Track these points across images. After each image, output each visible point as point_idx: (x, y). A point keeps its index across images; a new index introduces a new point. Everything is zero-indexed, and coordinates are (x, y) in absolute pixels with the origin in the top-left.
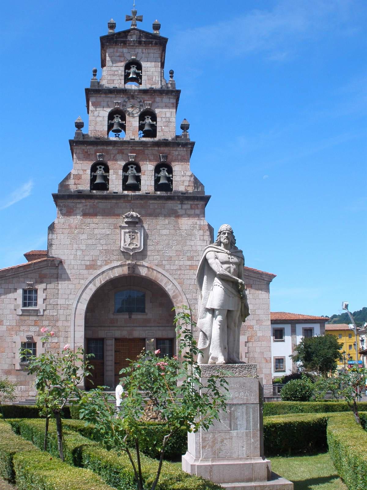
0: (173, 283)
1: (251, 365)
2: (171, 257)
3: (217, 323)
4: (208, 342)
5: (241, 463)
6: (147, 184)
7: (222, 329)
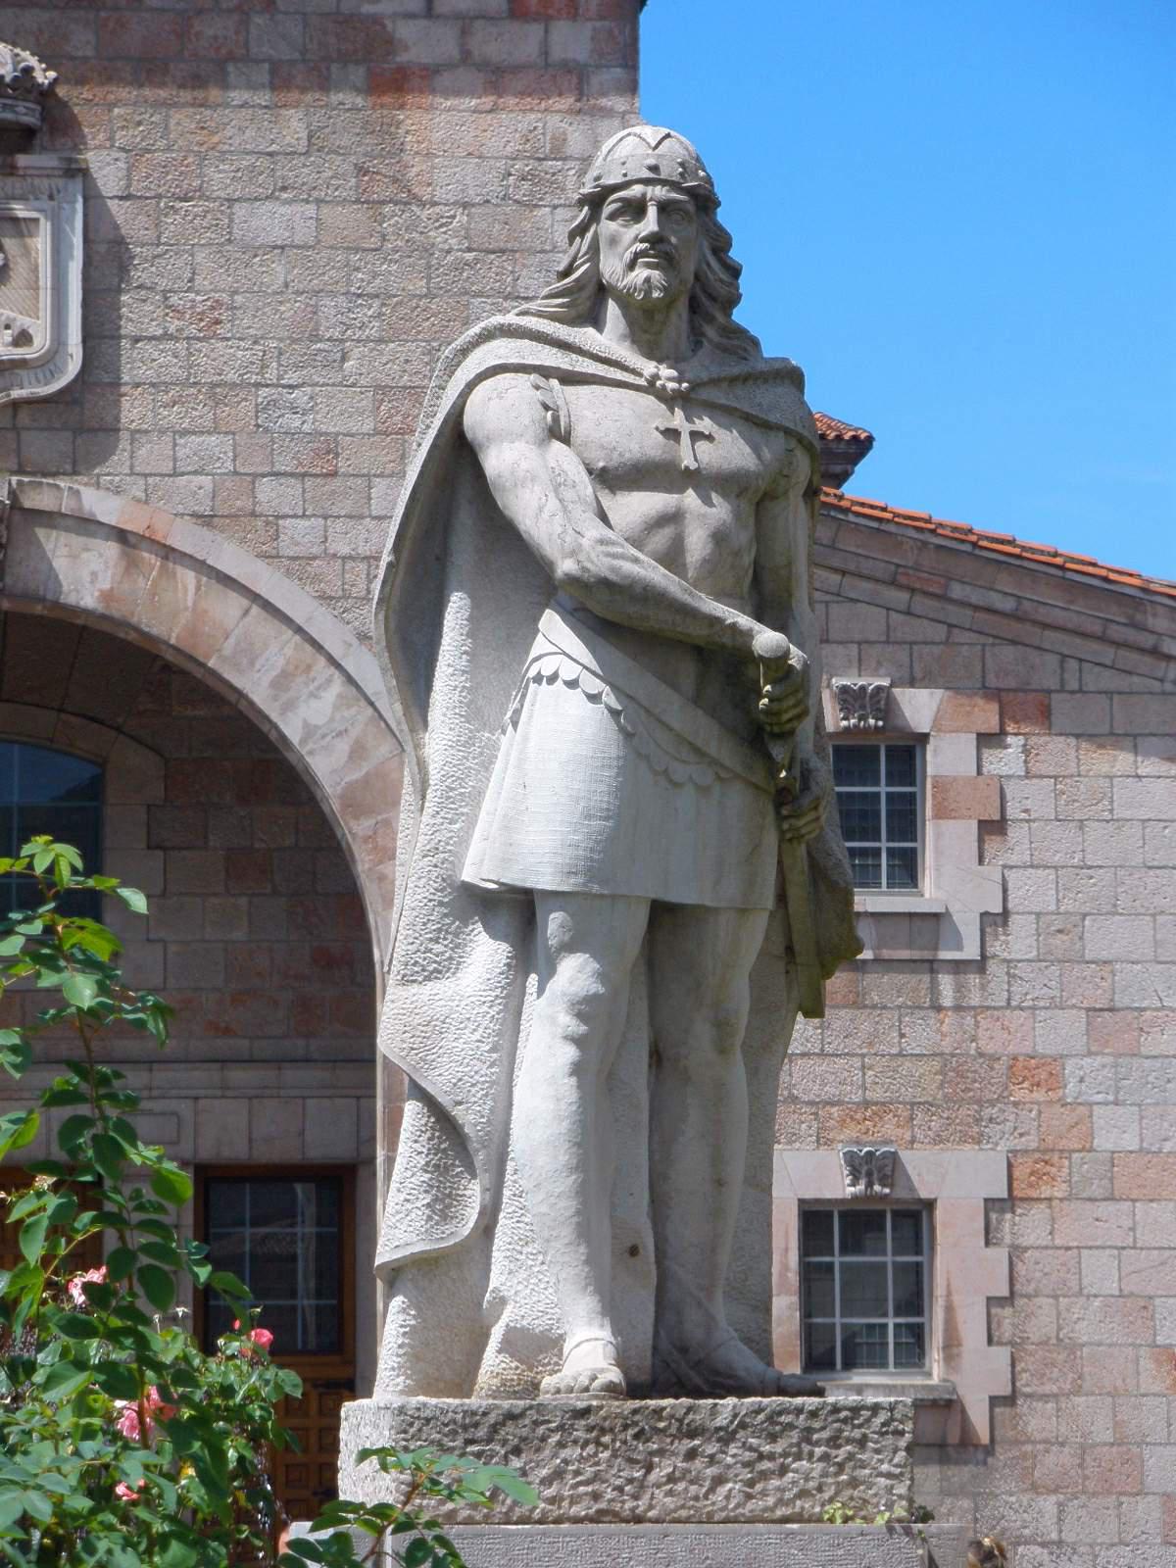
0: (350, 680)
1: (856, 1410)
2: (329, 447)
3: (553, 1020)
4: (474, 1193)
7: (596, 1072)
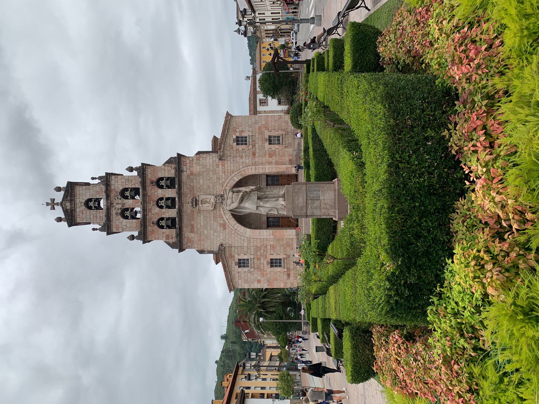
6: (171, 193)
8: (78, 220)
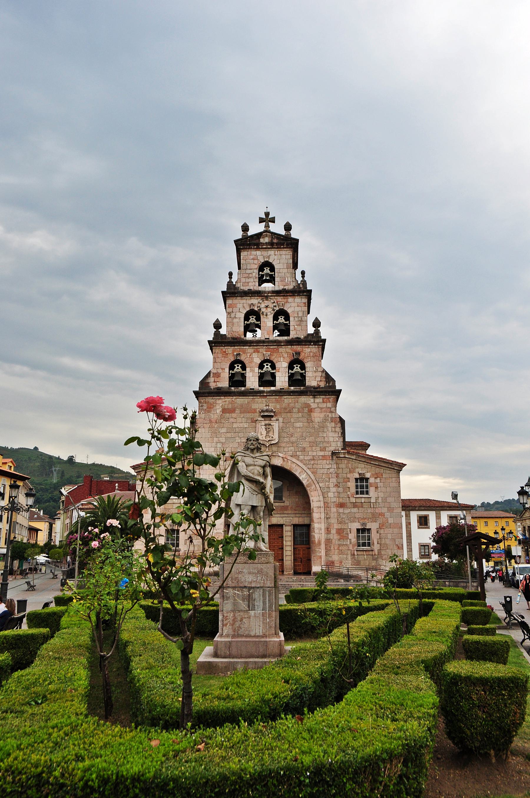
2: (304, 448)
5: (257, 640)
6: (282, 380)
8: (243, 254)
